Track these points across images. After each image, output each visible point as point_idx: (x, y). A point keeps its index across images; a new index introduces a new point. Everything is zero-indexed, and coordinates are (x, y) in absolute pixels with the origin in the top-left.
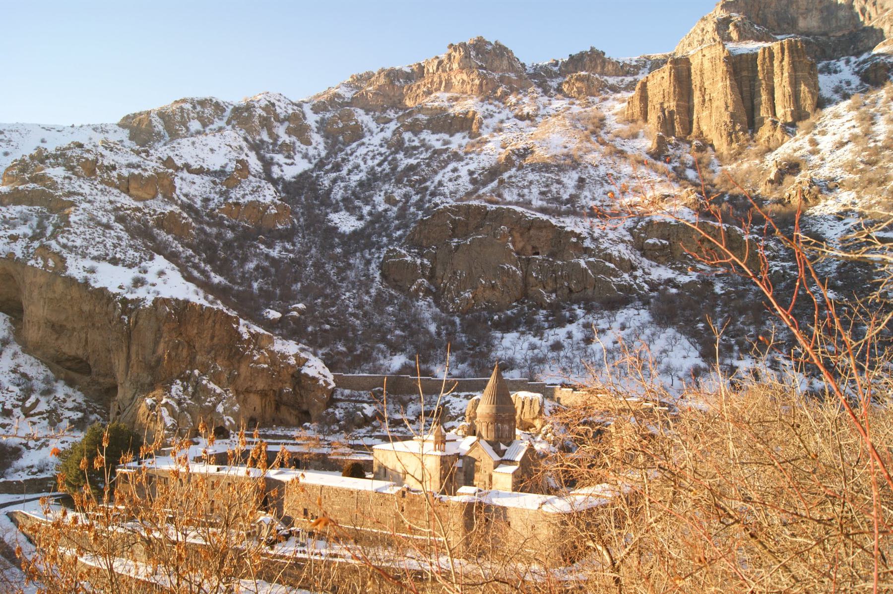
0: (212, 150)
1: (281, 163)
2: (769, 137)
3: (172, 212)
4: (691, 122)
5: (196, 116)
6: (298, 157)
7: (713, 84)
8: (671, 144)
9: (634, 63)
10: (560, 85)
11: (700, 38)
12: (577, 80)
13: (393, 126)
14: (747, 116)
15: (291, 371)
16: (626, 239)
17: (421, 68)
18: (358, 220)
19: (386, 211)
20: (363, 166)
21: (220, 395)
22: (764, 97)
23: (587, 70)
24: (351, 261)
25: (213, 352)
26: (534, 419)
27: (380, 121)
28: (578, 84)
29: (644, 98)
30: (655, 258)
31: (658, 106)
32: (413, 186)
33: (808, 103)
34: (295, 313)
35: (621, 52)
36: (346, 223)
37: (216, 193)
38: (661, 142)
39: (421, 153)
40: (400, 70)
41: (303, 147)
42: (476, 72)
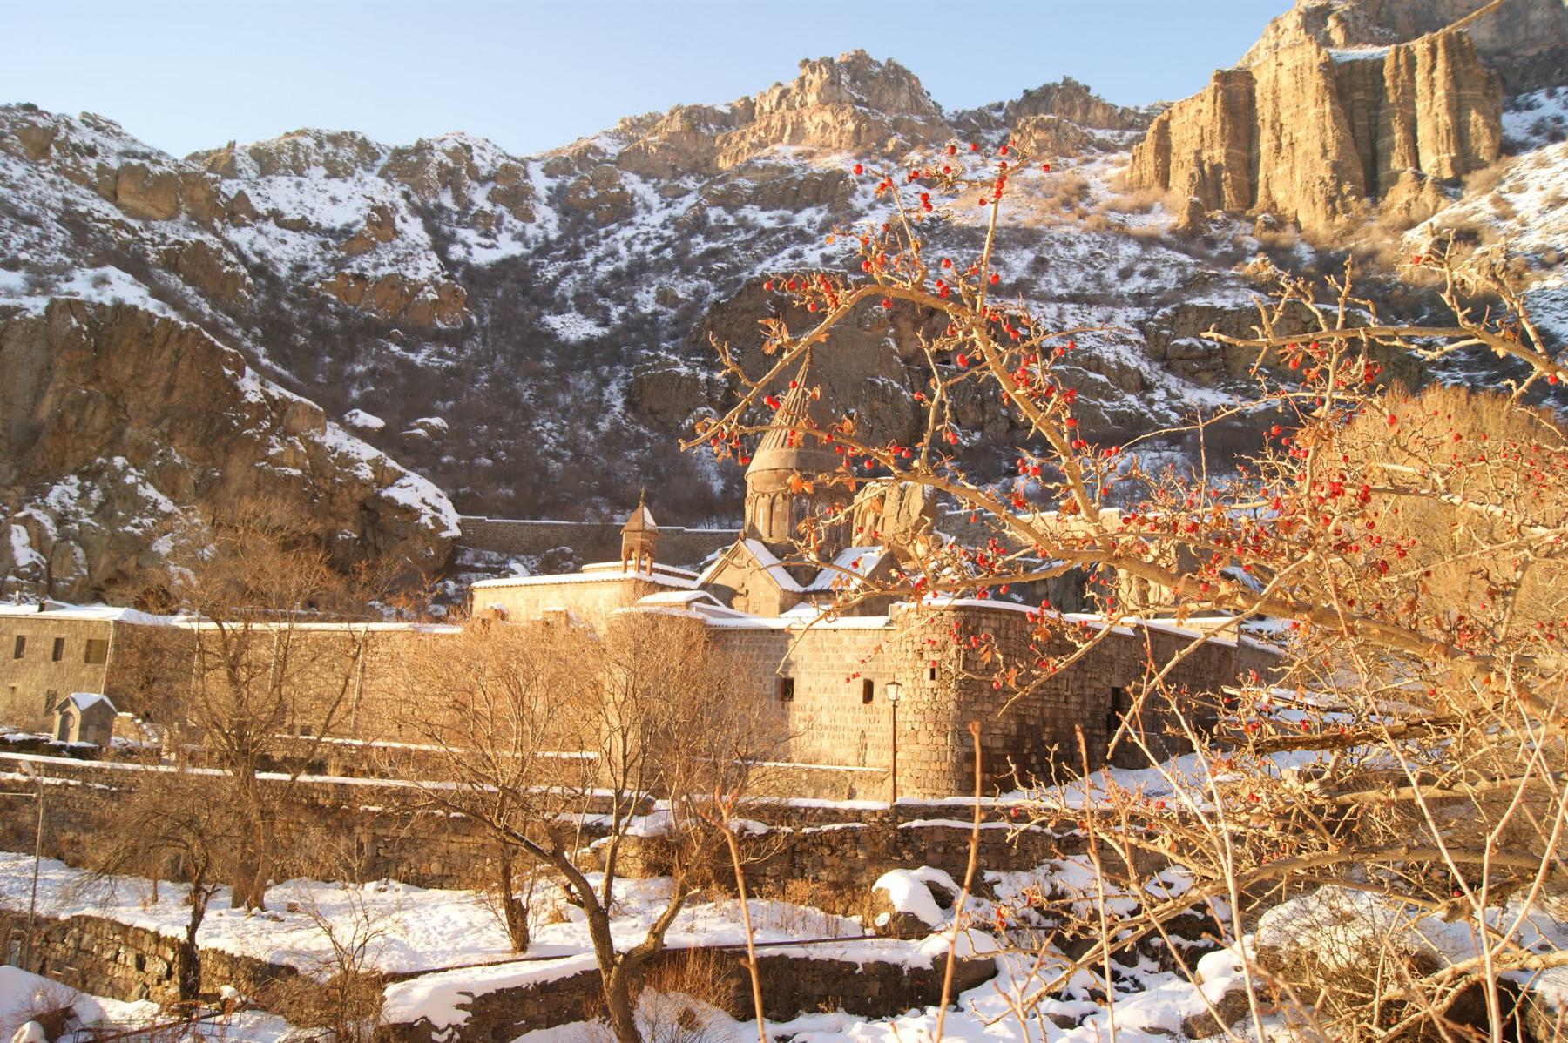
0: (334, 200)
2: (1408, 203)
3: (200, 243)
4: (1253, 188)
5: (322, 160)
8: (1215, 222)
9: (1142, 111)
11: (1273, 43)
12: (1036, 126)
13: (690, 200)
14: (1364, 166)
16: (1132, 337)
17: (749, 105)
19: (655, 314)
20: (623, 251)
21: (168, 516)
22: (1398, 136)
23: (1059, 113)
24: (571, 381)
25: (166, 422)
27: (668, 193)
28: (1038, 135)
29: (1163, 149)
31: (1192, 157)
32: (713, 279)
33: (1483, 146)
34: (421, 431)
36: (574, 327)
37: (324, 260)
38: (1196, 211)
40: (712, 109)
41: (519, 224)
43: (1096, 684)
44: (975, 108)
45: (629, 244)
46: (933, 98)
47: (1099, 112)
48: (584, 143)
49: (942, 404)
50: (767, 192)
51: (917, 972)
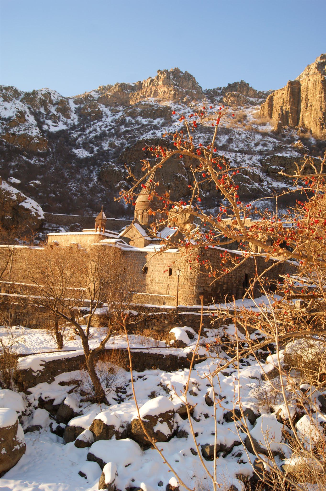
0: (5, 109)
1: (49, 124)
4: (298, 119)
6: (60, 124)
7: (313, 97)
8: (285, 129)
9: (265, 93)
10: (222, 99)
11: (307, 73)
12: (231, 96)
13: (120, 114)
15: (12, 204)
16: (257, 165)
18: (90, 153)
19: (108, 150)
20: (98, 129)
23: (239, 92)
24: (81, 171)
26: (185, 223)
27: (113, 111)
29: (271, 105)
30: (275, 177)
31: (279, 108)
32: (127, 140)
34: (32, 185)
35: (258, 85)
36: (82, 153)
38: (280, 126)
39: (135, 126)
40: (128, 85)
41: (65, 119)
42: (173, 87)
43: (240, 272)
44: (212, 89)
45: (100, 127)
46: (199, 85)
47: (251, 92)
48: (87, 94)
49: (197, 188)
50: (145, 112)
51: (182, 358)
